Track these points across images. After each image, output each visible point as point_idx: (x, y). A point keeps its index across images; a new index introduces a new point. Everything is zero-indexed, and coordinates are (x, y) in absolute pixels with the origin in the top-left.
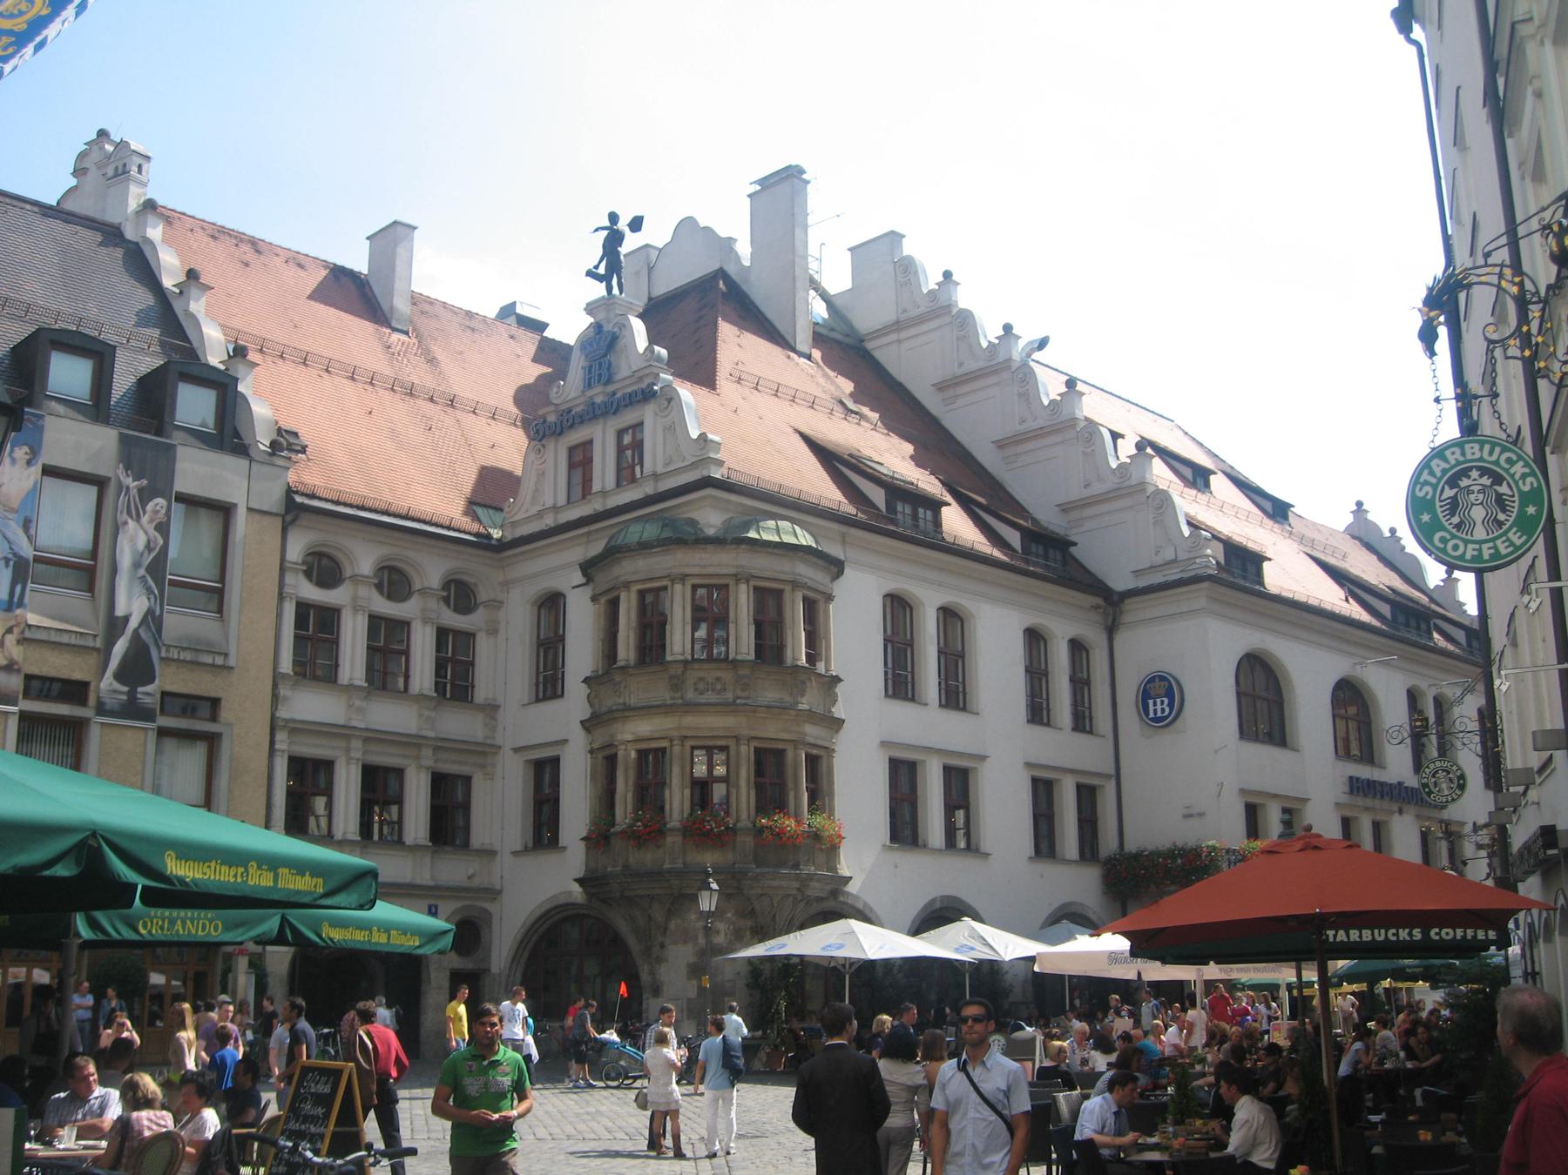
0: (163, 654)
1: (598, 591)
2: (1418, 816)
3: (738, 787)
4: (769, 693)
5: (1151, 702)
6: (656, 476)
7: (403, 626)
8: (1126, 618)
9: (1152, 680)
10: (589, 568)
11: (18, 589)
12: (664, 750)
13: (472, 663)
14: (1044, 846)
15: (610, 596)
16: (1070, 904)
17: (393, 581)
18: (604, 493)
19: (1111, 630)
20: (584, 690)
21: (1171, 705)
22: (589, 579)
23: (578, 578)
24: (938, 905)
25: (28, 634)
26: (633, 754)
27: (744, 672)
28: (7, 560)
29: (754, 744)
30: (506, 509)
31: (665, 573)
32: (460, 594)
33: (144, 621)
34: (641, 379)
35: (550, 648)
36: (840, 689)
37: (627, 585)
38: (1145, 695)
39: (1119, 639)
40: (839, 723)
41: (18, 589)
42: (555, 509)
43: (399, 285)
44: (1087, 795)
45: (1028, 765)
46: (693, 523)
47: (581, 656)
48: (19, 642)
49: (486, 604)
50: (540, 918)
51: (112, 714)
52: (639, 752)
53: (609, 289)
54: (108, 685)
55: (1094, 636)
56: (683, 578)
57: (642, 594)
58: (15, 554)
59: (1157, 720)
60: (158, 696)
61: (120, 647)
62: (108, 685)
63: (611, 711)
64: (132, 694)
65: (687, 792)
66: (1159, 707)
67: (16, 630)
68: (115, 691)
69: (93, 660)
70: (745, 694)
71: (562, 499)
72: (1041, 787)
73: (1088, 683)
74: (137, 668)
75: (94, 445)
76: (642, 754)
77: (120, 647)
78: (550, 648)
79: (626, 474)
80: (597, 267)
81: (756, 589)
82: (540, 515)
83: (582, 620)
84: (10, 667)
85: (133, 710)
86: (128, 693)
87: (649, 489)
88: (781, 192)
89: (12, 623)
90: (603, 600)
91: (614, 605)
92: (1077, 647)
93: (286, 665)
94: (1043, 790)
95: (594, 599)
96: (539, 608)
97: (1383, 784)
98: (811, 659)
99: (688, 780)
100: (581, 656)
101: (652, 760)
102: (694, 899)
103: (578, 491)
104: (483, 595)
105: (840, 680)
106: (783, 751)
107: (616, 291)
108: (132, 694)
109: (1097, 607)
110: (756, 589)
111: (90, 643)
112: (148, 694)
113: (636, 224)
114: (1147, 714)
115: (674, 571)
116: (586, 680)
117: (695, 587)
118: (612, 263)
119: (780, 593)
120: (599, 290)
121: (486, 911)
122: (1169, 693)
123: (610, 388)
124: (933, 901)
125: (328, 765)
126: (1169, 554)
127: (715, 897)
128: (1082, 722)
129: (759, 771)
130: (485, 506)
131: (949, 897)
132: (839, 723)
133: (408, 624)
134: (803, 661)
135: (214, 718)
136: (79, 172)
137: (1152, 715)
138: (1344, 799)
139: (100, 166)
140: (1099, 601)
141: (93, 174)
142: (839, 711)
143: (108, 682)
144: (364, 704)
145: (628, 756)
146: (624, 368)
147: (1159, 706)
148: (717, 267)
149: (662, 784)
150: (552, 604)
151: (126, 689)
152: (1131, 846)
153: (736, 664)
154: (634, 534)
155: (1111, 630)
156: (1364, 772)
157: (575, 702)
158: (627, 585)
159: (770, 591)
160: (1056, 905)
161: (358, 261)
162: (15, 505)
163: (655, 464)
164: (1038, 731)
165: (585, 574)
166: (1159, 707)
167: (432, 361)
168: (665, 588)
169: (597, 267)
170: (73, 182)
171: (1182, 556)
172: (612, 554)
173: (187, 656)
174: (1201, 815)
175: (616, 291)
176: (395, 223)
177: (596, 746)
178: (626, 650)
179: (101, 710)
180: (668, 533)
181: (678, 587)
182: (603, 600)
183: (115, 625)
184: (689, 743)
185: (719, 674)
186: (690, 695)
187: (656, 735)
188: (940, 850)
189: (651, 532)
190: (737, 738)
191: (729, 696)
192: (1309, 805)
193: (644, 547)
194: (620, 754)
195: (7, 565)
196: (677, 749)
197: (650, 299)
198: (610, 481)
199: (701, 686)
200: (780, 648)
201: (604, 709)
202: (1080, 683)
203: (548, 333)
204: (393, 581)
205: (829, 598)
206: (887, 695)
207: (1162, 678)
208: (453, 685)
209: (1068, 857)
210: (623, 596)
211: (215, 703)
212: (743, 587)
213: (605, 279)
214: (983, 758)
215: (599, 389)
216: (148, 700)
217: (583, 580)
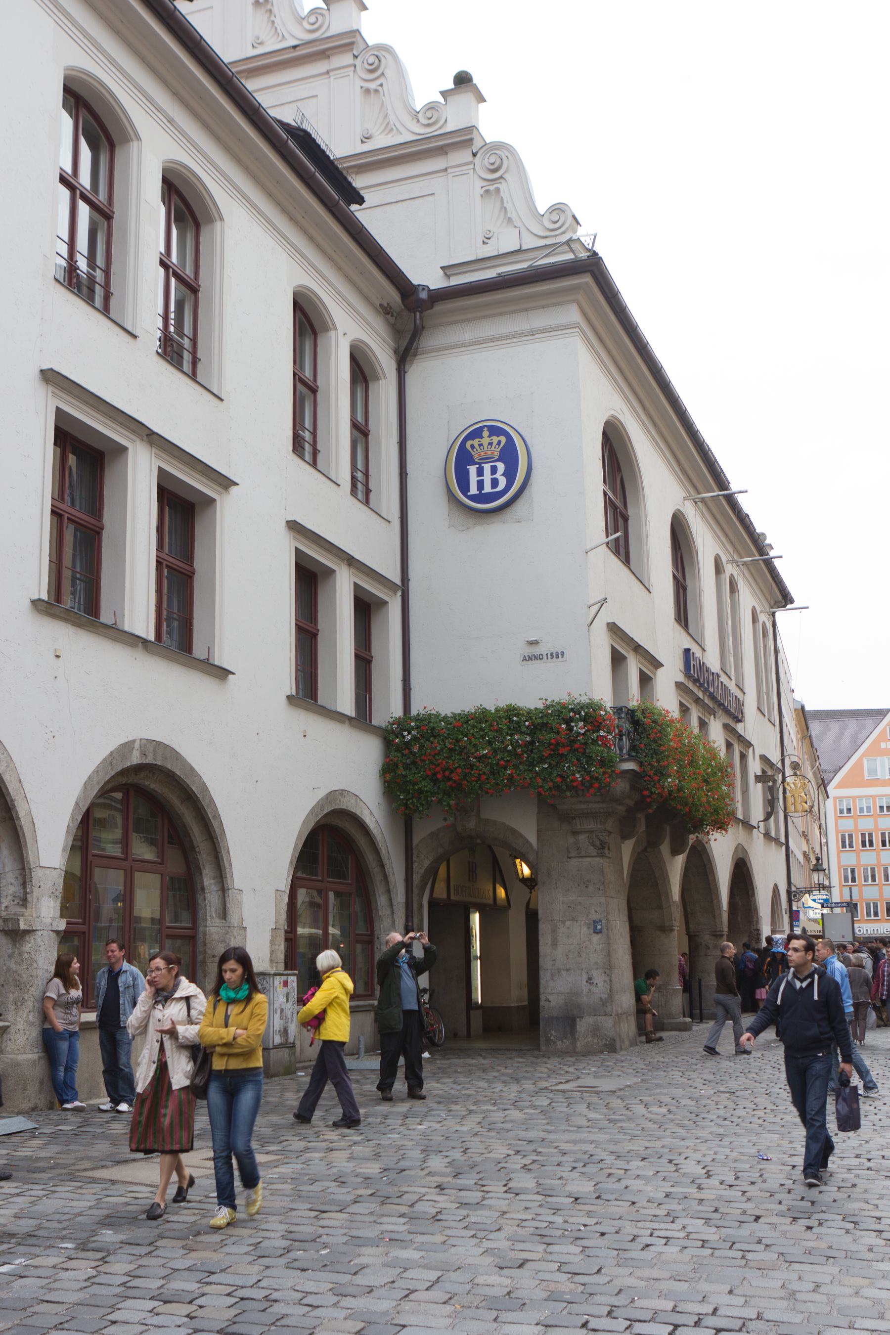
2: (726, 726)
5: (473, 469)
8: (429, 340)
9: (476, 433)
16: (342, 792)
19: (404, 357)
21: (510, 475)
24: (136, 759)
38: (464, 459)
39: (416, 372)
44: (365, 609)
45: (294, 527)
55: (384, 358)
59: (481, 498)
66: (487, 478)
94: (309, 579)
97: (708, 670)
109: (386, 311)
122: (509, 455)
124: (128, 746)
126: (507, 242)
128: (362, 487)
131: (159, 743)
137: (473, 490)
138: (681, 678)
147: (487, 477)
152: (416, 709)
155: (404, 357)
156: (695, 649)
160: (321, 794)
166: (487, 478)
171: (530, 242)
174: (557, 655)
188: (145, 642)
192: (660, 671)
202: (361, 431)
207: (495, 431)
209: (339, 710)
214: (226, 483)
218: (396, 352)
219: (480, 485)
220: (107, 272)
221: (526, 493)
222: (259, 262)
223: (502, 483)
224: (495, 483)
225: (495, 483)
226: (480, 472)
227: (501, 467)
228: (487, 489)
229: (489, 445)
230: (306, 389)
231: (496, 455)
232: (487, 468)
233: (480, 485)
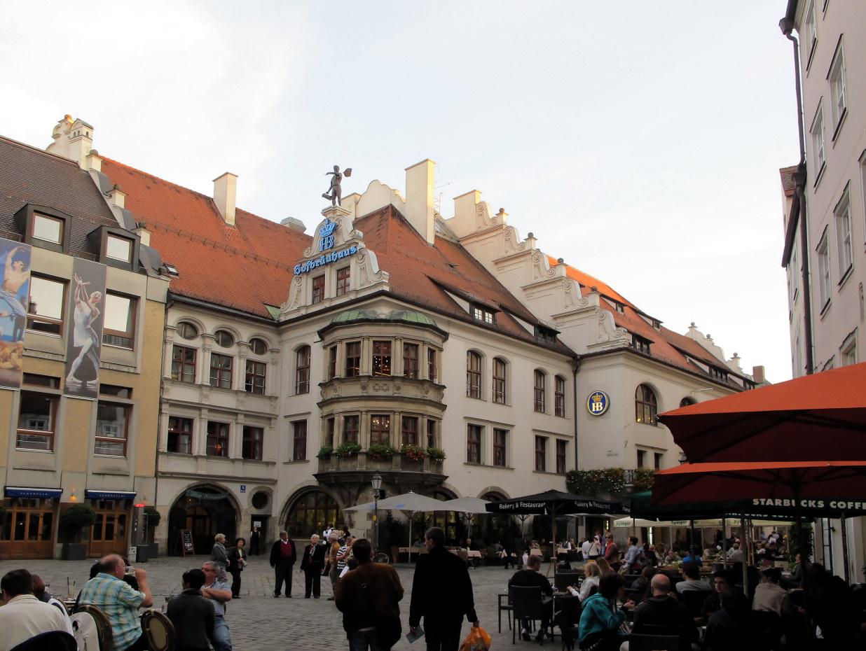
0: (101, 366)
1: (326, 344)
3: (394, 433)
4: (410, 391)
5: (593, 404)
6: (357, 291)
7: (230, 359)
9: (595, 394)
10: (322, 334)
11: (19, 331)
12: (358, 416)
13: (264, 377)
14: (540, 467)
15: (332, 346)
17: (226, 338)
18: (331, 300)
19: (575, 372)
20: (319, 389)
21: (604, 406)
22: (322, 339)
23: (317, 338)
25: (25, 353)
26: (342, 418)
27: (398, 382)
28: (12, 317)
29: (402, 415)
30: (282, 307)
31: (360, 335)
32: (259, 345)
33: (90, 350)
34: (349, 246)
35: (303, 372)
36: (445, 392)
37: (341, 341)
38: (591, 401)
39: (578, 376)
40: (445, 406)
41: (19, 331)
42: (307, 307)
43: (228, 203)
46: (374, 313)
47: (318, 373)
48: (19, 357)
49: (272, 351)
50: (296, 492)
51: (72, 393)
52: (345, 417)
53: (334, 203)
54: (71, 380)
56: (369, 338)
57: (349, 345)
58: (17, 314)
59: (595, 412)
60: (99, 386)
61: (78, 361)
62: (71, 380)
63: (332, 399)
64: (84, 385)
65: (369, 436)
66: (597, 407)
67: (17, 351)
68: (75, 383)
69: (63, 366)
70: (397, 392)
71: (310, 303)
72: (539, 439)
73: (563, 395)
74: (86, 372)
75: (64, 264)
76: (347, 418)
77: (78, 361)
78: (303, 372)
79: (343, 289)
80: (327, 193)
81: (405, 343)
82: (299, 309)
83: (318, 359)
84: (15, 369)
85: (84, 392)
86: (82, 384)
87: (353, 297)
88: (418, 170)
89: (16, 347)
90: (329, 348)
91: (334, 350)
92: (559, 379)
93: (168, 373)
95: (325, 347)
96: (298, 353)
98: (432, 376)
99: (369, 430)
100: (318, 373)
101: (352, 421)
102: (370, 484)
103: (318, 299)
104: (270, 347)
105: (446, 387)
106: (417, 418)
107: (337, 204)
108: (84, 385)
110: (405, 343)
111: (60, 358)
112: (93, 384)
113: (348, 173)
114: (591, 409)
115: (364, 335)
116: (320, 385)
117: (374, 342)
118: (335, 193)
119: (417, 346)
120: (329, 203)
121: (270, 489)
123: (334, 250)
125: (189, 422)
127: (380, 482)
129: (405, 425)
130: (272, 306)
132: (445, 406)
133: (232, 358)
134: (427, 378)
135: (129, 396)
136: (56, 136)
137: (594, 410)
139: (67, 133)
140: (570, 358)
141: (63, 138)
142: (444, 402)
143: (71, 378)
144: (208, 393)
145: (339, 420)
146: (340, 241)
147: (597, 406)
148: (386, 203)
149: (356, 432)
150: (304, 350)
151: (81, 382)
153: (394, 378)
154: (345, 316)
155: (575, 372)
157: (315, 394)
158: (341, 341)
159: (412, 345)
161: (209, 191)
162: (16, 290)
163: (355, 285)
164: (539, 416)
165: (320, 336)
166: (597, 407)
167: (246, 239)
168: (360, 342)
169: (327, 193)
170: (53, 141)
172: (333, 327)
173: (115, 367)
175: (337, 204)
176: (227, 173)
177: (324, 415)
178: (340, 371)
179: (67, 391)
180: (361, 317)
181: (366, 342)
182: (329, 348)
183: (74, 351)
184: (369, 414)
185: (385, 382)
186: (371, 392)
187: (354, 409)
189: (353, 316)
190: (394, 412)
191: (390, 393)
193: (349, 324)
194: (336, 418)
195: (12, 319)
196: (364, 416)
197: (356, 219)
198: (334, 295)
199: (377, 387)
200: (416, 372)
201: (329, 398)
202: (560, 397)
203: (306, 233)
204: (226, 338)
205: (441, 350)
206: (467, 396)
207: (600, 394)
208: (254, 386)
210: (339, 346)
211: (130, 390)
212: (398, 342)
213: (332, 198)
215: (330, 250)
216: (92, 387)
217: (320, 339)
218: (573, 371)
219: (596, 408)
220: (480, 387)
221: (607, 413)
222: (522, 367)
223: (602, 408)
224: (599, 408)
225: (599, 408)
226: (596, 405)
227: (601, 404)
228: (597, 410)
229: (597, 398)
230: (539, 392)
231: (600, 400)
232: (597, 404)
233: (596, 408)
